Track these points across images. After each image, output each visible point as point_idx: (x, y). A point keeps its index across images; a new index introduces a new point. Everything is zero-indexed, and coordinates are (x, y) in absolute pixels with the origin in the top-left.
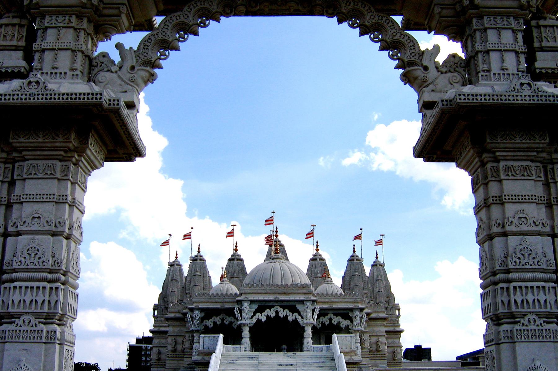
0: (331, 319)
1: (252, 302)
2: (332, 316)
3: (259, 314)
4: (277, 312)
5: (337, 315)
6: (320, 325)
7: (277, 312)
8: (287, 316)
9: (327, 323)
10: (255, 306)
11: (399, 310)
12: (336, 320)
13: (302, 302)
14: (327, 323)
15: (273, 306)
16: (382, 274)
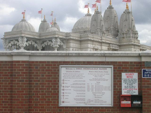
0: (48, 43)
1: (6, 39)
2: (48, 42)
3: (9, 44)
4: (14, 42)
5: (49, 41)
6: (44, 46)
7: (14, 42)
8: (17, 44)
9: (46, 45)
10: (8, 41)
11: (138, 34)
12: (49, 43)
13: (18, 37)
14: (46, 45)
15: (13, 40)
16: (128, 17)
